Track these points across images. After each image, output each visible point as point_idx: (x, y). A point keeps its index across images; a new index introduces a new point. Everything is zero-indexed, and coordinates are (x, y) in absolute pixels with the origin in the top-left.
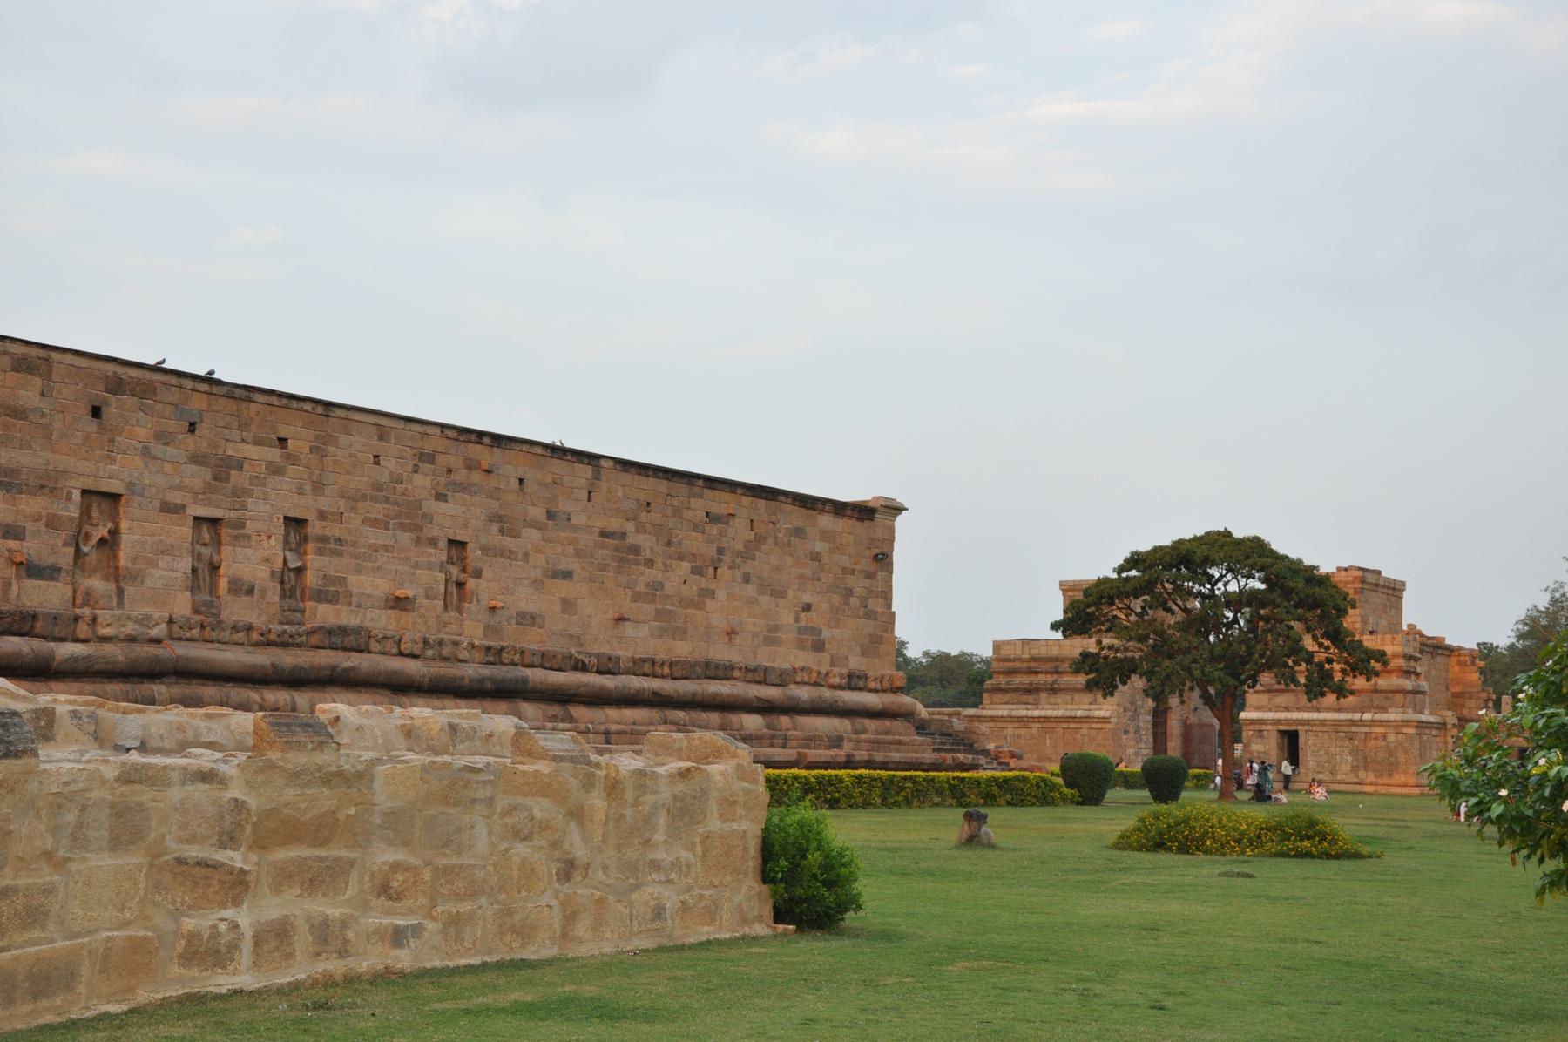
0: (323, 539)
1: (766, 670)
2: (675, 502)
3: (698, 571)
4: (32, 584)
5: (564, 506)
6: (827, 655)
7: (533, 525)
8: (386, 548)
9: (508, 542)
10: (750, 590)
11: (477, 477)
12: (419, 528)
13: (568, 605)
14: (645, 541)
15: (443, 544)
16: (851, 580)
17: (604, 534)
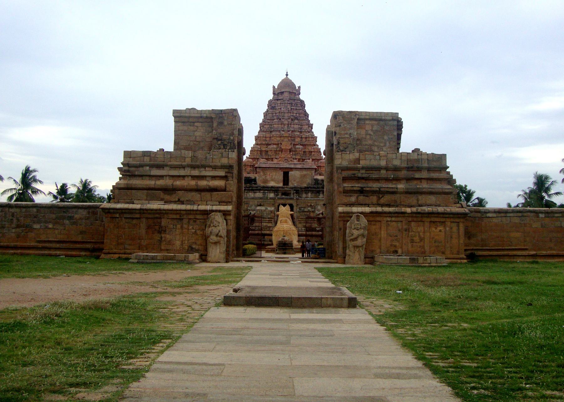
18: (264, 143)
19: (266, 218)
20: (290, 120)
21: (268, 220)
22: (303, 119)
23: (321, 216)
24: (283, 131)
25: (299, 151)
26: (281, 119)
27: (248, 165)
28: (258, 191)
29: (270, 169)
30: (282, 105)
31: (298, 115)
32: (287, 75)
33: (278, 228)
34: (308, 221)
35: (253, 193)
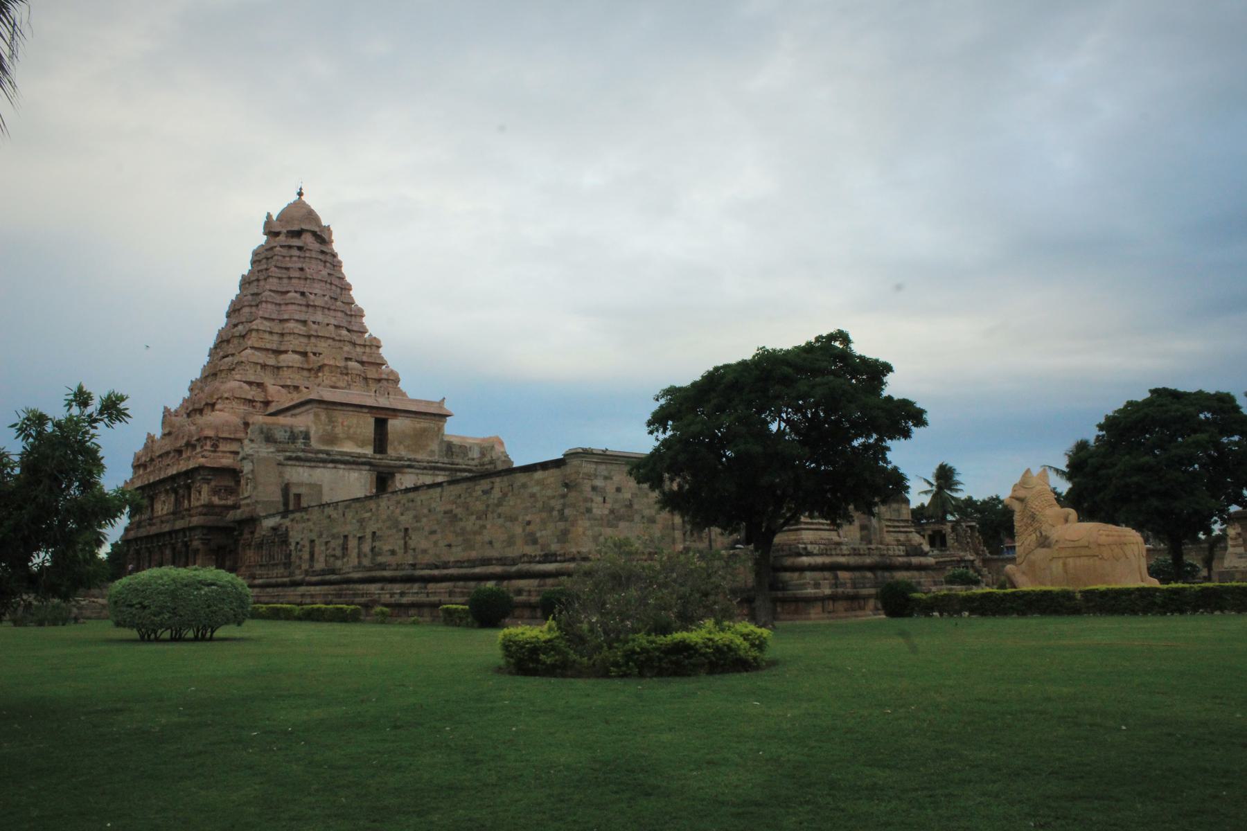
0: (378, 537)
1: (506, 558)
2: (469, 490)
3: (479, 518)
4: (337, 562)
5: (433, 505)
6: (538, 546)
7: (425, 516)
8: (391, 535)
9: (419, 524)
10: (501, 521)
11: (410, 504)
12: (397, 527)
13: (436, 543)
14: (459, 511)
15: (403, 530)
16: (553, 502)
17: (445, 513)
18: (268, 346)
24: (314, 323)
25: (357, 375)
27: (237, 398)
28: (321, 465)
29: (344, 408)
32: (300, 194)
35: (307, 470)
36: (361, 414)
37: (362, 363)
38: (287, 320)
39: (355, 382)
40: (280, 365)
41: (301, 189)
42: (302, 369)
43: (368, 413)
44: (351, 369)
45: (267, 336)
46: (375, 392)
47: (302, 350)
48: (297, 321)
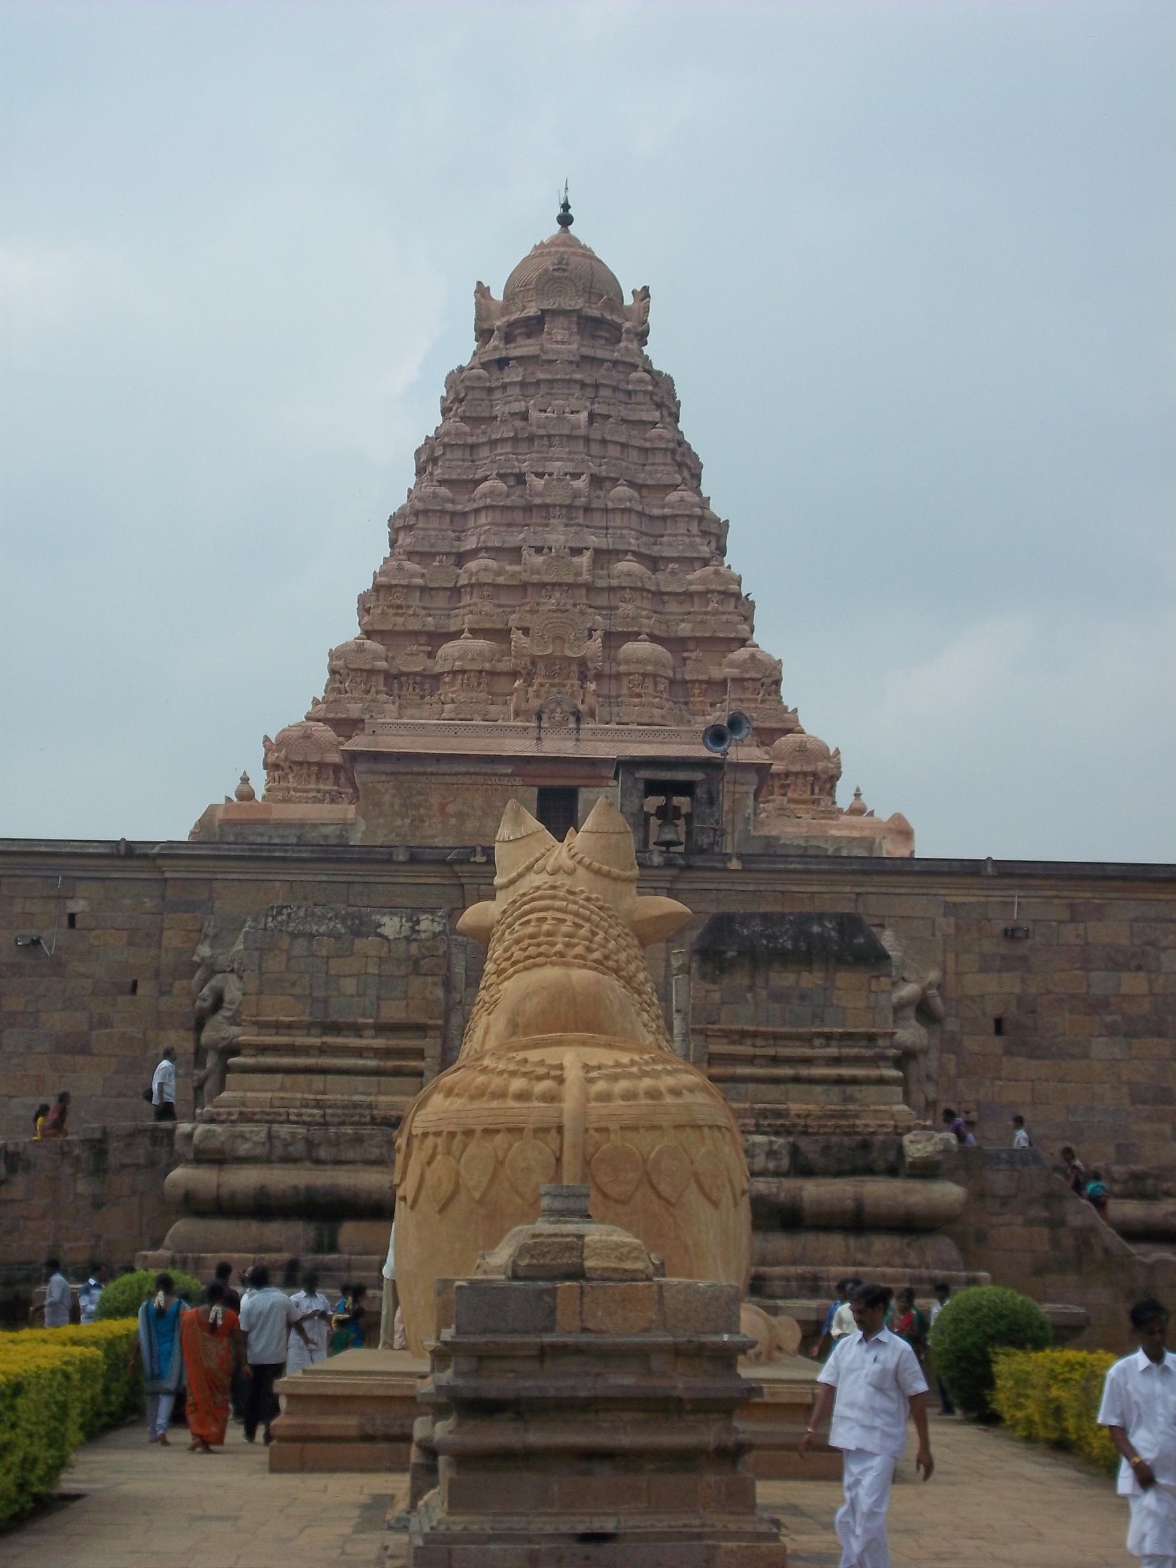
18: (415, 626)
19: (357, 1030)
20: (581, 484)
21: (379, 1043)
22: (666, 480)
23: (910, 1033)
24: (539, 550)
25: (645, 675)
26: (531, 478)
27: (301, 764)
29: (444, 768)
30: (531, 391)
31: (634, 454)
32: (565, 220)
33: (480, 1094)
34: (808, 1061)
36: (495, 780)
37: (676, 643)
38: (473, 553)
39: (639, 696)
40: (438, 669)
41: (566, 207)
42: (492, 674)
43: (512, 775)
44: (627, 662)
45: (415, 600)
46: (540, 718)
47: (499, 626)
48: (496, 552)
